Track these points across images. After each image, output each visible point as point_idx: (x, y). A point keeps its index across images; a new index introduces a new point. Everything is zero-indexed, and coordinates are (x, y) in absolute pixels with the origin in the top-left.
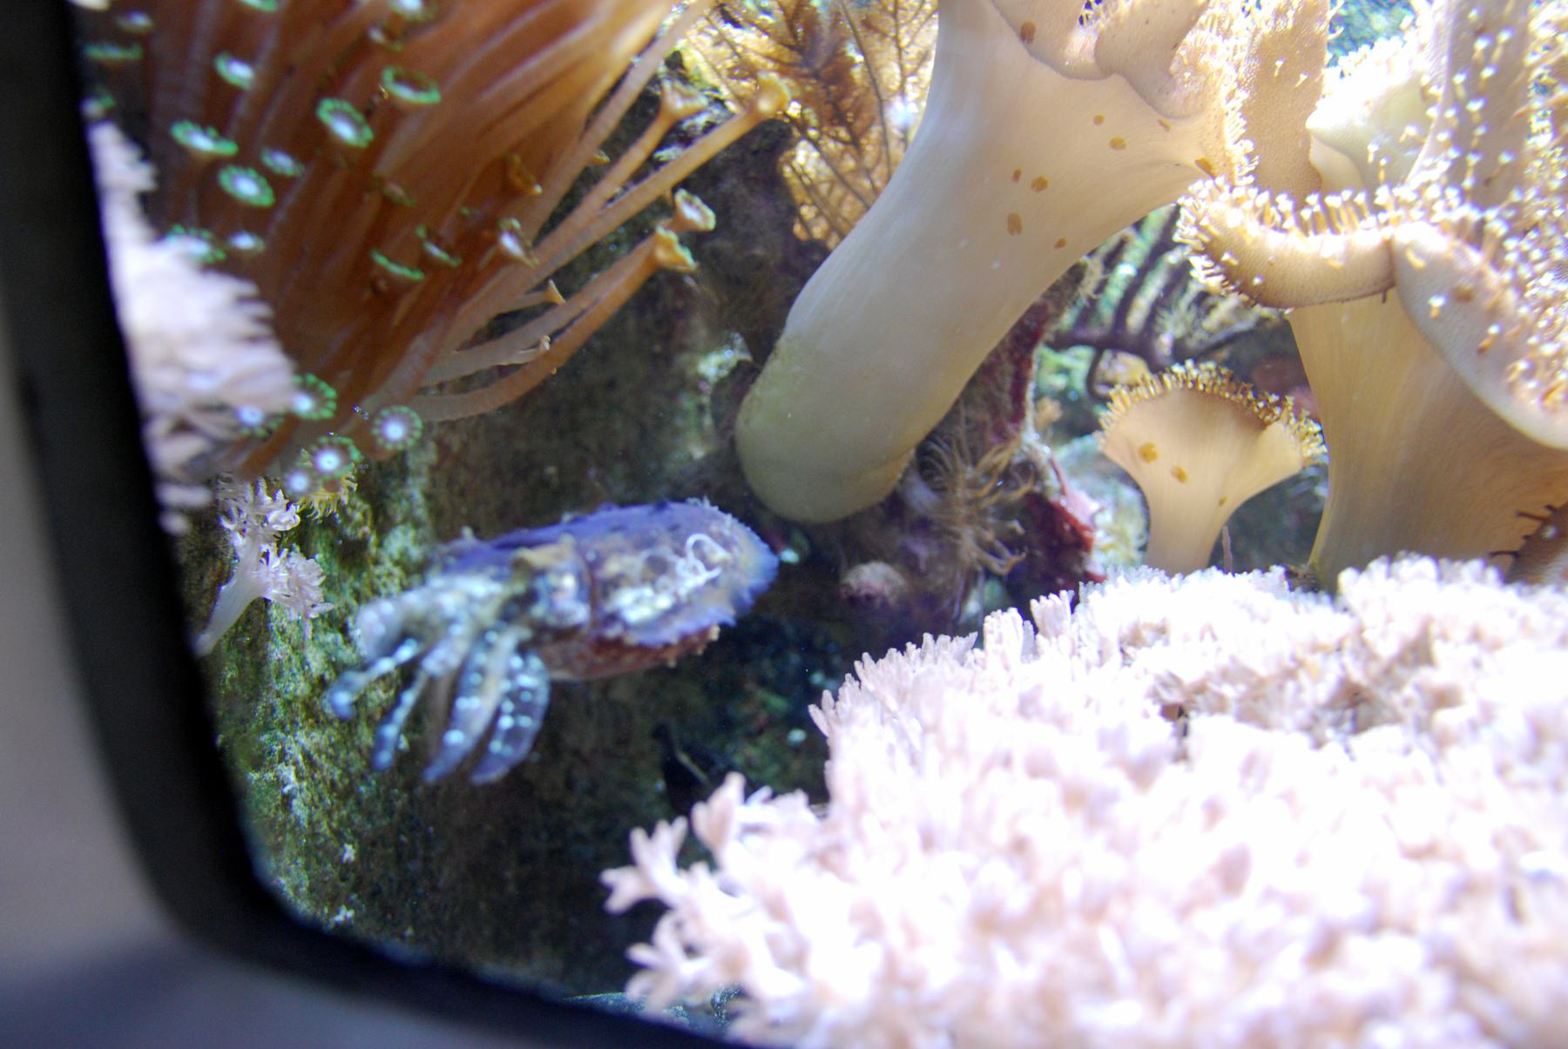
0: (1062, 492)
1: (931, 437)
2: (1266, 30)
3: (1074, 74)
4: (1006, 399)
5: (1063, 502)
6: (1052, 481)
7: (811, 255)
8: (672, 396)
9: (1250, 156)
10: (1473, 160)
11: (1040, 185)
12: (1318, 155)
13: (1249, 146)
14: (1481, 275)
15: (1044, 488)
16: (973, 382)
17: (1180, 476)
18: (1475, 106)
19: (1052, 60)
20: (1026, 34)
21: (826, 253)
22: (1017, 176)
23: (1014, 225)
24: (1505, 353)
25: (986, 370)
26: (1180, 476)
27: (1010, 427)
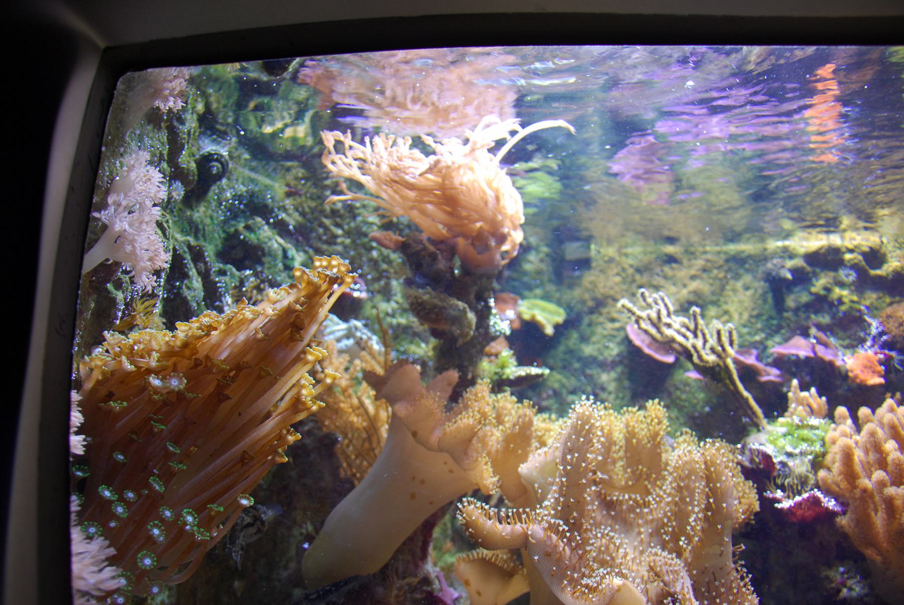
0: (441, 590)
1: (386, 567)
2: (509, 431)
3: (430, 449)
4: (418, 551)
5: (440, 595)
6: (436, 585)
7: (346, 486)
8: (290, 528)
9: (498, 481)
10: (562, 499)
11: (423, 482)
12: (523, 482)
13: (496, 479)
14: (556, 546)
15: (433, 589)
16: (404, 543)
17: (479, 594)
18: (564, 480)
19: (425, 444)
20: (414, 434)
21: (353, 487)
22: (414, 478)
23: (413, 496)
24: (561, 575)
25: (411, 539)
26: (479, 594)
27: (420, 563)
